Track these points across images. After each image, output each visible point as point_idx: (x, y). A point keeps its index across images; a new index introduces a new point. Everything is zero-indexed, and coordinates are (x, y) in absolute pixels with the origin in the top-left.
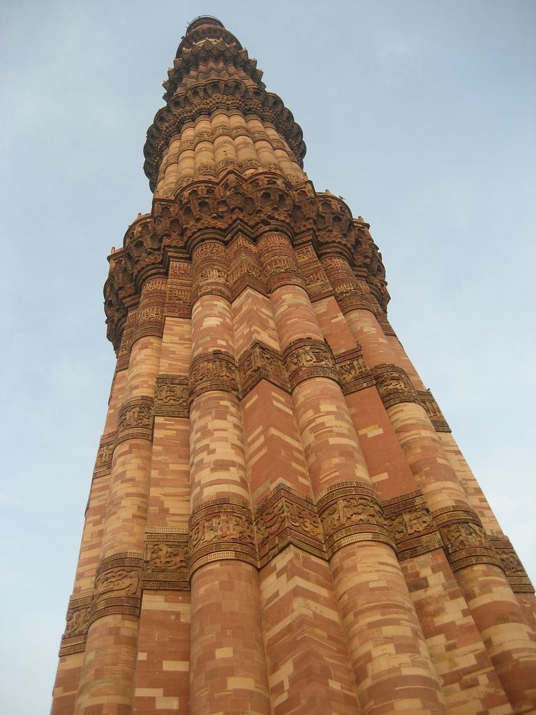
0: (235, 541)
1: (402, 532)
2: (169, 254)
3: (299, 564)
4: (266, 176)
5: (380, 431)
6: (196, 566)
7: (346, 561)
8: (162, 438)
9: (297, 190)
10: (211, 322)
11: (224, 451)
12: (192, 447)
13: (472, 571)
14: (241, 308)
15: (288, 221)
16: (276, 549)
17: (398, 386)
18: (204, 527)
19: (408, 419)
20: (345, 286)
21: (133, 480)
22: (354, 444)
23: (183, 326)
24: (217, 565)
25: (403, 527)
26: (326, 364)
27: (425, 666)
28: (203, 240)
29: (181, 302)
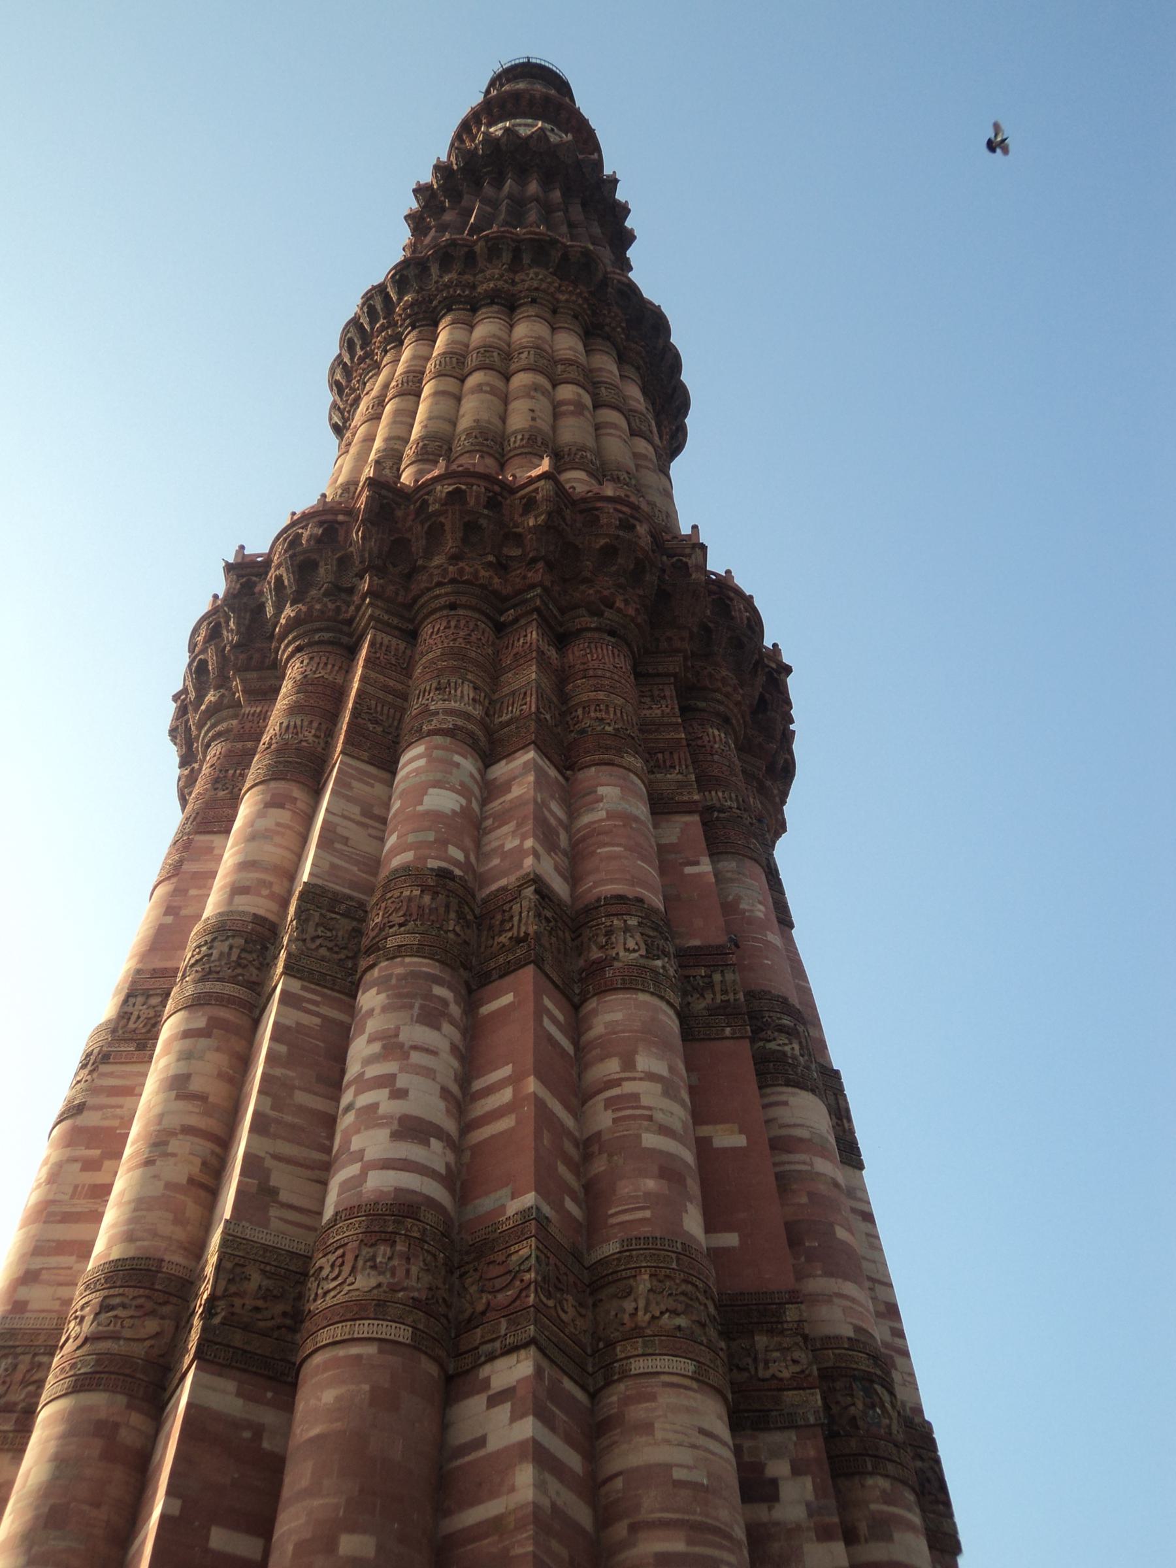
0: (416, 1304)
1: (746, 1370)
4: (619, 507)
5: (741, 1141)
6: (324, 1337)
7: (632, 1408)
8: (288, 1028)
9: (670, 556)
10: (444, 801)
11: (425, 1101)
12: (353, 1069)
13: (863, 1486)
14: (506, 787)
15: (639, 620)
16: (497, 1344)
17: (787, 1048)
18: (357, 1257)
19: (795, 1125)
20: (720, 794)
21: (202, 1098)
22: (689, 1157)
23: (372, 786)
24: (371, 1350)
25: (750, 1361)
26: (664, 967)
28: (453, 606)
29: (379, 729)
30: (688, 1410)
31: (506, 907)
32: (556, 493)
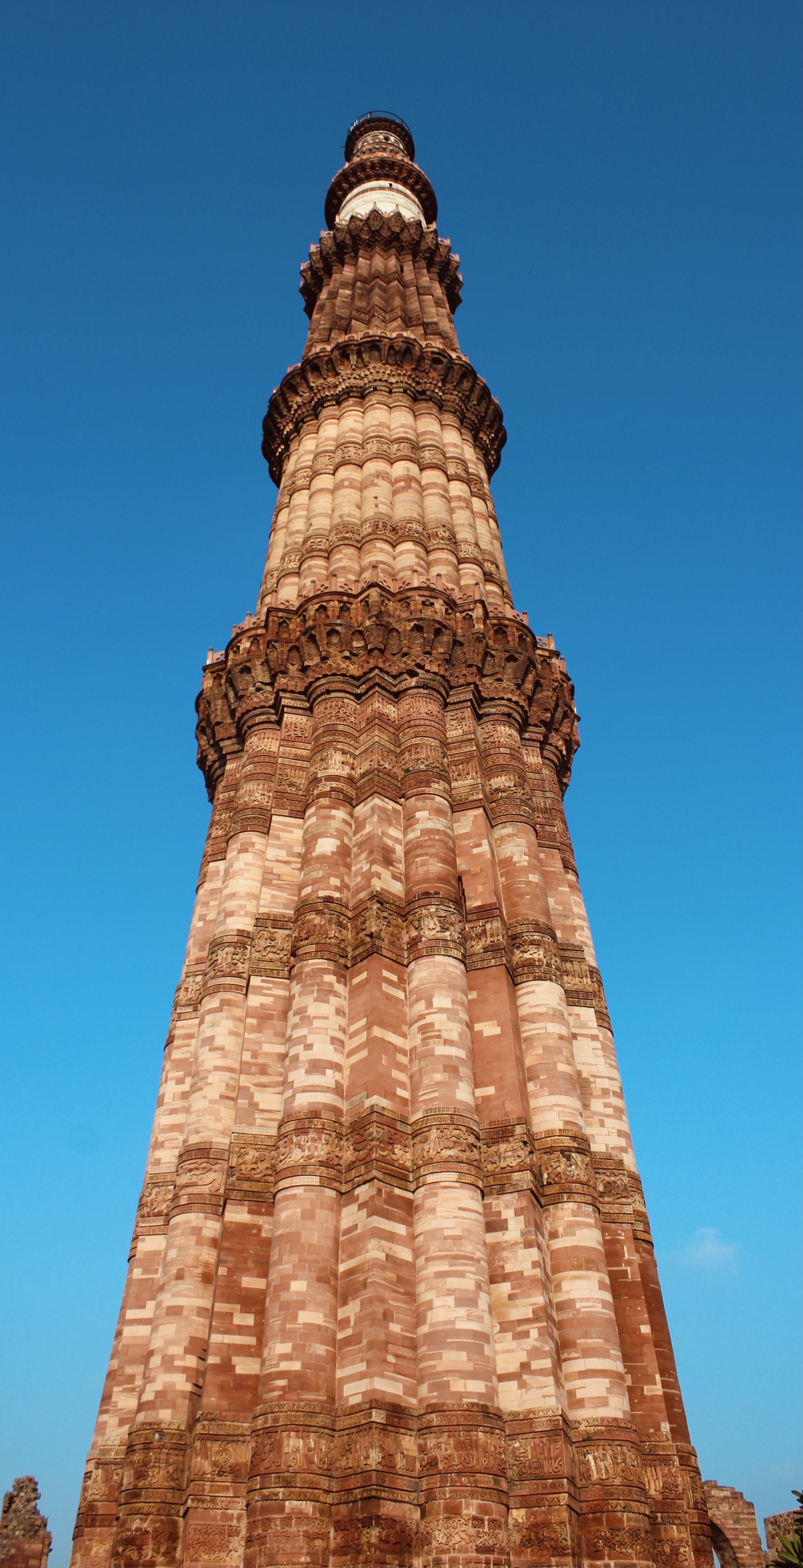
0: (322, 1164)
2: (284, 702)
3: (380, 1203)
4: (421, 593)
5: (497, 1031)
6: (282, 1184)
8: (256, 1008)
10: (327, 846)
12: (289, 1032)
15: (442, 673)
17: (536, 956)
19: (537, 1006)
23: (292, 832)
25: (496, 1158)
27: (480, 1319)
28: (328, 692)
30: (454, 1199)
31: (363, 914)
32: (381, 595)
